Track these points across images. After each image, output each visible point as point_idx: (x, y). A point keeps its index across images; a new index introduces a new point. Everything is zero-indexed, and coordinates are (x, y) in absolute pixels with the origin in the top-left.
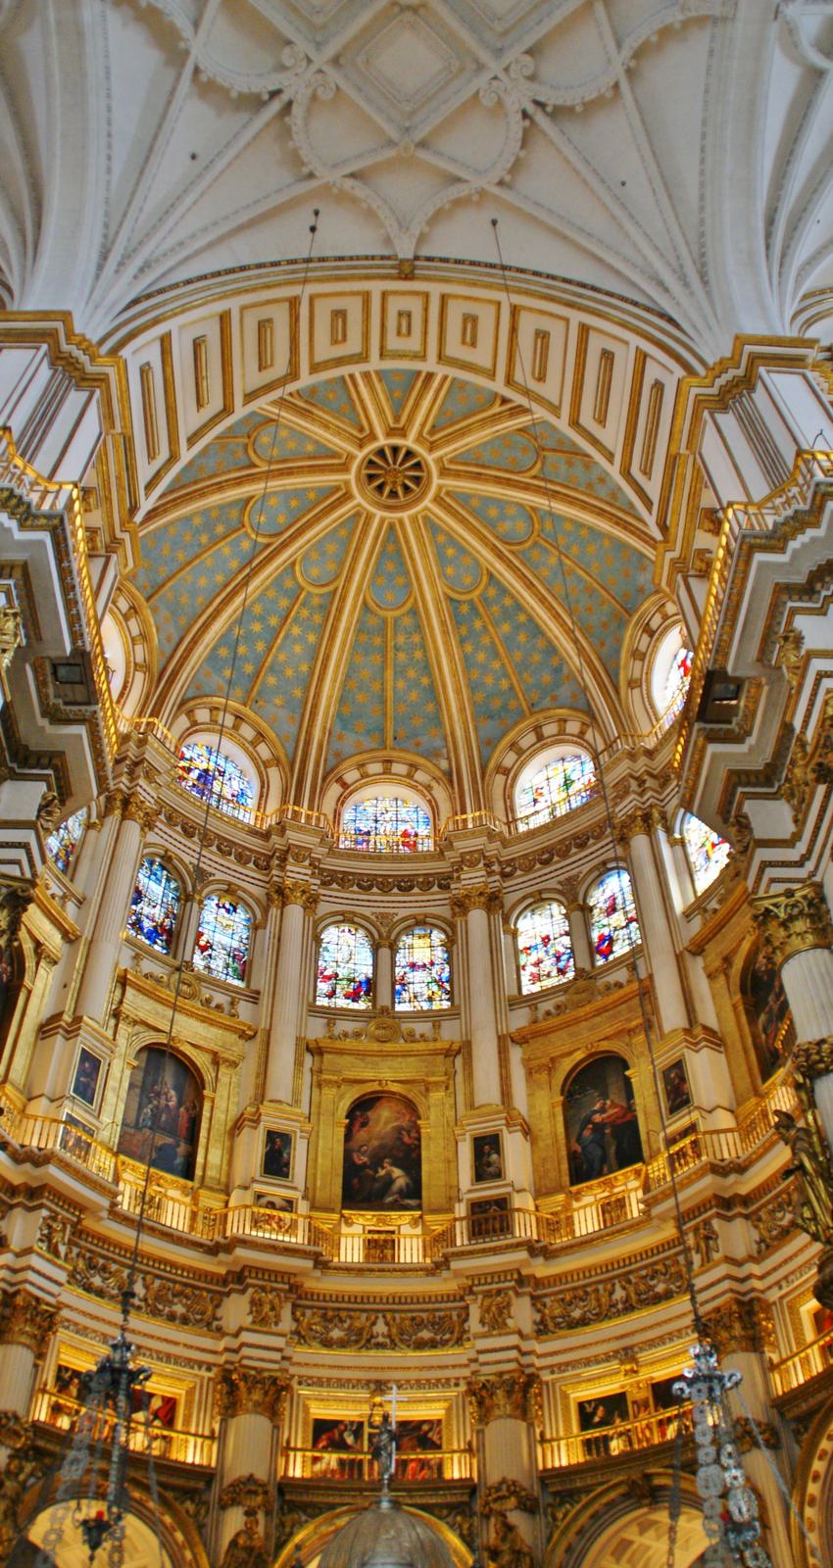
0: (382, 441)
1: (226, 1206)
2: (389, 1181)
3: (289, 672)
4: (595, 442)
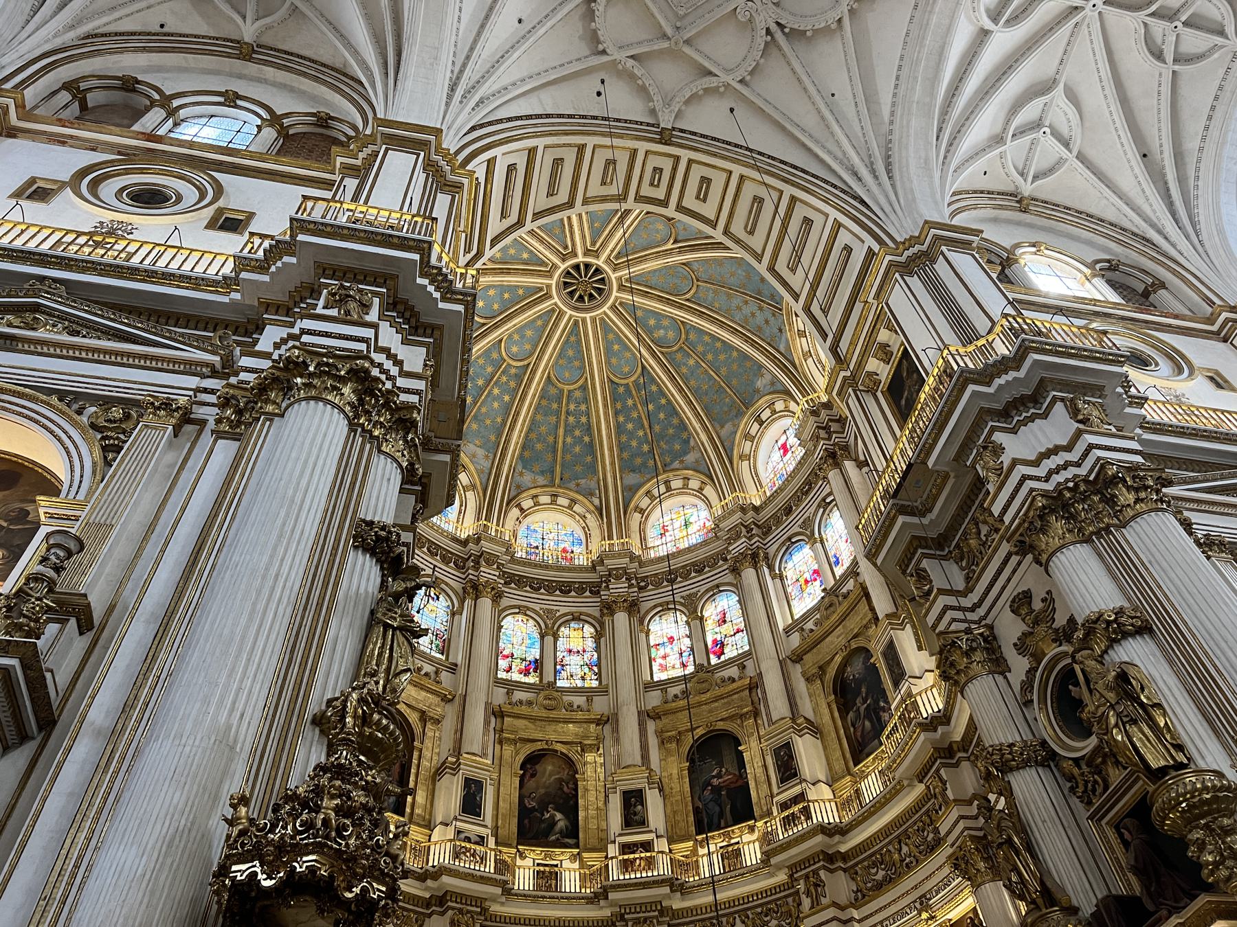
0: (581, 259)
1: (429, 841)
3: (488, 422)
4: (785, 284)
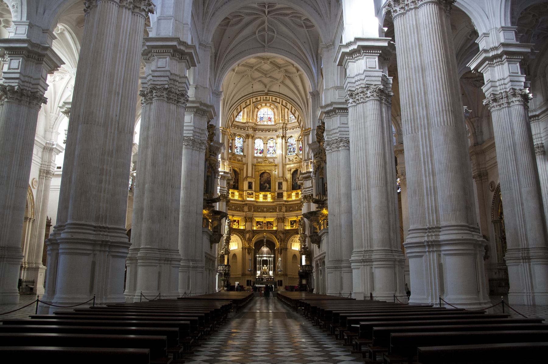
2: (266, 186)
